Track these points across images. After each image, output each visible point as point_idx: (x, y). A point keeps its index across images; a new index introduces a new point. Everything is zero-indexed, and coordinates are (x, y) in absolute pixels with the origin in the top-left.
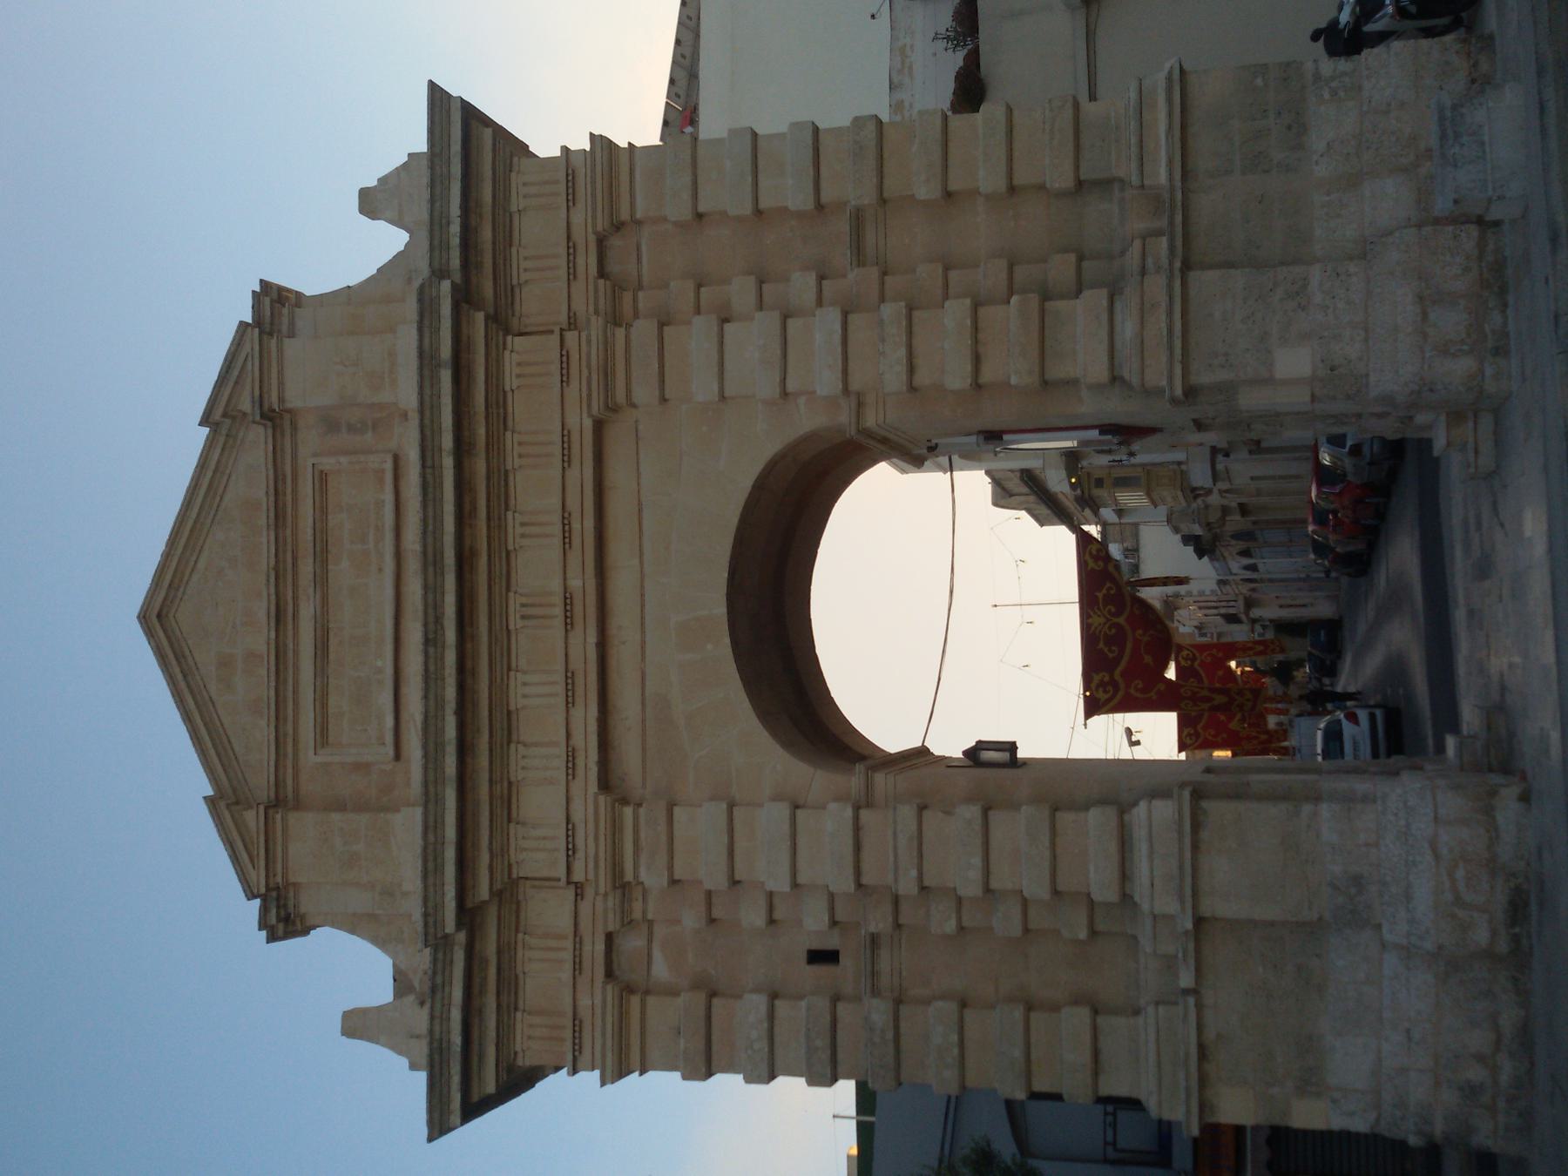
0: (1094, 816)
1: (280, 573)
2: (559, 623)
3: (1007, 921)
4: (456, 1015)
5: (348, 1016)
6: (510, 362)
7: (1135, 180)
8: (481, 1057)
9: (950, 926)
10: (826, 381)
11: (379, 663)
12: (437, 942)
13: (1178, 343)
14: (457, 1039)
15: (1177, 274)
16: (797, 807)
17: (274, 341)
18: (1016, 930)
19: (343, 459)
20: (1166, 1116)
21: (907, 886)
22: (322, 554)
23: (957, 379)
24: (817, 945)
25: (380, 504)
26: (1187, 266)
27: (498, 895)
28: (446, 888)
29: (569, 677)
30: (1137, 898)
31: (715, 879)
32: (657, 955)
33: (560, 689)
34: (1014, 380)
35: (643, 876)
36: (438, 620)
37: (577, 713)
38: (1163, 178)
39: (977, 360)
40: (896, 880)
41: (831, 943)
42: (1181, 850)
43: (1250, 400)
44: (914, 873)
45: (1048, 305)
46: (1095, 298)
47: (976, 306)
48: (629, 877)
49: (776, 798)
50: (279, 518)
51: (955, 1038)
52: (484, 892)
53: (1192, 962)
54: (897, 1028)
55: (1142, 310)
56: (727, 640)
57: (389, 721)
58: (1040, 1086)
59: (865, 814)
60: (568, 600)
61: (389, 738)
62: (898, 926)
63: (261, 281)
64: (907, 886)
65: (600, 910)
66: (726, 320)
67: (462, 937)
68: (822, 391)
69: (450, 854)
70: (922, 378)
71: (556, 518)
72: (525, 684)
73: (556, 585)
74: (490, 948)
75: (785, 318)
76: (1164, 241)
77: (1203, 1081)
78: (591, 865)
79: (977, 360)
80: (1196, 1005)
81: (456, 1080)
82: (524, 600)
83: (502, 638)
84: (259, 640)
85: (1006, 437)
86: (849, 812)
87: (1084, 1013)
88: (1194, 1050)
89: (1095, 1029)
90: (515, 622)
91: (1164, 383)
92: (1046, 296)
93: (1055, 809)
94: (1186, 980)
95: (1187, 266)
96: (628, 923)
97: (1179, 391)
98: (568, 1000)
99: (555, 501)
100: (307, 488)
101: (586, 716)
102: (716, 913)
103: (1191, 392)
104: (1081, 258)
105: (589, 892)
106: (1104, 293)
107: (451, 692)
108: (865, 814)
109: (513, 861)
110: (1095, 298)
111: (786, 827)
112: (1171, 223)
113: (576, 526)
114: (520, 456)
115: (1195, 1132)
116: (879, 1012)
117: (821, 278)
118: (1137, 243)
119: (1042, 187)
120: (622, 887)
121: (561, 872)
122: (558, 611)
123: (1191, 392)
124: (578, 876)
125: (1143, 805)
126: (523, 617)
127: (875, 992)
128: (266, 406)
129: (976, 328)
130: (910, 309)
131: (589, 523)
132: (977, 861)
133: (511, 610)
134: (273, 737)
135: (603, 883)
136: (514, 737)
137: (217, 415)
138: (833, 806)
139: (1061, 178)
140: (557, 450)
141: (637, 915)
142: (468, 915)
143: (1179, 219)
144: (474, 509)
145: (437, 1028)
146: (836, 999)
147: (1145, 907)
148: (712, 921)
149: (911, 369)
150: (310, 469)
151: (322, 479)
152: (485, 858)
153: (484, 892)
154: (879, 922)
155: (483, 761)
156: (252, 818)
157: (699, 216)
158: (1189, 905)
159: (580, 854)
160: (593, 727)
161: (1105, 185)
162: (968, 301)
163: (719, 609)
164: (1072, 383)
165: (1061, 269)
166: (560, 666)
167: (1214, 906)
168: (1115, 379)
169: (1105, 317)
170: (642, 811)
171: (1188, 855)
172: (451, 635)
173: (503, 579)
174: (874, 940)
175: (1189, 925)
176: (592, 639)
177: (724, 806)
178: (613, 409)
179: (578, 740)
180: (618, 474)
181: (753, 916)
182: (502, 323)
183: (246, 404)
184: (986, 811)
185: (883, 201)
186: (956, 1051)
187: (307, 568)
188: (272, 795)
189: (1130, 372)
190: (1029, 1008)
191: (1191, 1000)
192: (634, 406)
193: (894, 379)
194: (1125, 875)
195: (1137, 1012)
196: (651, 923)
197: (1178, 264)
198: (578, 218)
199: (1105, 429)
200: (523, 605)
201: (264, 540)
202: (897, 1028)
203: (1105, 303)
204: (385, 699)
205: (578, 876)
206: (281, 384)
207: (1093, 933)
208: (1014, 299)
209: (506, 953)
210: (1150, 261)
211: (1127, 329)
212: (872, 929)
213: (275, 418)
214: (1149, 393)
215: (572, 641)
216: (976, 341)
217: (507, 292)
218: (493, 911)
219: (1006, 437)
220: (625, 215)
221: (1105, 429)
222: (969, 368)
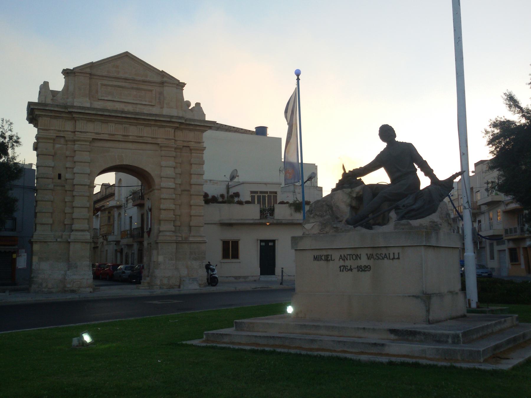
0: (88, 226)
1: (134, 80)
2: (124, 134)
3: (68, 210)
4: (52, 109)
5: (48, 83)
6: (170, 129)
7: (191, 235)
8: (42, 112)
9: (66, 200)
10: (163, 185)
11: (116, 97)
12: (66, 107)
13: (165, 241)
14: (47, 108)
15: (176, 241)
16: (89, 175)
17: (175, 86)
18: (66, 212)
19: (154, 96)
20: (34, 236)
21: (75, 193)
22: (138, 89)
23: (162, 206)
24: (62, 175)
25: (146, 101)
26: (177, 243)
27: (74, 118)
28: (77, 110)
29: (114, 135)
30: (73, 232)
31: (76, 159)
32: (60, 146)
33: (112, 133)
34: (161, 215)
35: (76, 146)
36: (126, 114)
37: (107, 136)
38: (190, 239)
39: (165, 210)
40: (76, 192)
41: (63, 178)
42: (82, 240)
43: (155, 252)
44: (77, 195)
45: (173, 221)
46: (173, 229)
47: (174, 210)
48: (76, 143)
49: (91, 171)
50: (144, 81)
51: (47, 200)
52: (74, 116)
53: (62, 241)
54: (48, 190)
55: (171, 236)
56: (119, 164)
57: (106, 99)
58: (38, 215)
59: (87, 187)
60: (128, 136)
61: (103, 98)
62: (66, 191)
63: (186, 84)
64: (75, 193)
65: (69, 136)
66: (174, 168)
67: (66, 111)
68: (162, 183)
69: (83, 111)
70: (162, 201)
71: (142, 135)
72: (113, 126)
73: (130, 134)
74: (63, 115)
75: (174, 178)
76: (181, 239)
77: (41, 242)
78: (79, 136)
79: (165, 210)
80: (54, 241)
81: (40, 108)
82: (128, 128)
83: (121, 123)
84: (121, 75)
85: (150, 212)
86: (88, 184)
87: (51, 222)
88: (47, 241)
89: (48, 224)
90: (124, 125)
91: (159, 239)
92: (174, 221)
93: (88, 219)
94: (59, 240)
95: (177, 243)
96: (66, 141)
97: (158, 241)
98: (53, 128)
99: (145, 135)
100: (150, 88)
101: (106, 137)
102: (68, 158)
103: (157, 243)
104: (179, 226)
105: (73, 134)
106: (173, 230)
107: (113, 114)
108: (87, 187)
109: (80, 121)
110: (173, 229)
111: (85, 173)
112: (184, 241)
113: (141, 139)
114: (153, 130)
115: (32, 240)
116: (51, 186)
117: (180, 184)
118: (180, 235)
119: (191, 221)
120: (74, 141)
121: (77, 130)
122: (126, 134)
123: (157, 243)
124: (76, 133)
125: (90, 234)
126: (125, 127)
127: (54, 186)
128: (165, 83)
129: (170, 210)
130: (174, 199)
131: (141, 141)
132: (79, 206)
133: (126, 125)
134: (103, 75)
135: (75, 138)
136: (103, 123)
137: (163, 73)
138: (89, 181)
139: (192, 224)
140: (154, 136)
141: (68, 143)
142: (70, 113)
143: (184, 242)
144: (145, 121)
145: (49, 105)
146: (52, 179)
147: (71, 234)
148: (67, 157)
149: (164, 199)
150: (153, 89)
151: (151, 91)
152: (81, 116)
153: (74, 116)
154: (68, 187)
155: (99, 118)
156: (88, 70)
157: (191, 164)
158: (73, 241)
159: (81, 134)
160: (104, 138)
161: (190, 230)
162: (174, 209)
163: (125, 163)
164: (160, 224)
165: (178, 223)
166: (116, 133)
167: (72, 245)
168: (160, 231)
169: (170, 230)
170: (89, 146)
171: (81, 241)
172: (124, 115)
173: (131, 124)
174: (64, 186)
175: (69, 241)
176: (120, 139)
177: (89, 162)
178: (161, 147)
179: (102, 135)
180: (149, 147)
181: (68, 165)
182: (177, 128)
183: (165, 79)
184: (88, 208)
185: (191, 195)
186: (44, 200)
187: (135, 86)
188: (92, 74)
189: (161, 234)
190: (51, 213)
191: (55, 241)
192: (161, 150)
193: (163, 196)
194: (76, 230)
195: (51, 231)
196: (67, 145)
197: (177, 242)
198: (193, 143)
199: (150, 229)
200: (127, 127)
201: (140, 78)
202: (48, 190)
203: (172, 230)
204: (110, 98)
205: (76, 133)
206: (168, 86)
207: (65, 225)
208: (174, 216)
209: (62, 118)
210: (178, 237)
211: (168, 233)
212: (66, 186)
213: (162, 83)
214: (158, 236)
215: (120, 136)
216: (168, 210)
217: (182, 129)
218: (70, 116)
219: (150, 212)
220: (193, 151)
221: (150, 229)
222: (164, 208)
